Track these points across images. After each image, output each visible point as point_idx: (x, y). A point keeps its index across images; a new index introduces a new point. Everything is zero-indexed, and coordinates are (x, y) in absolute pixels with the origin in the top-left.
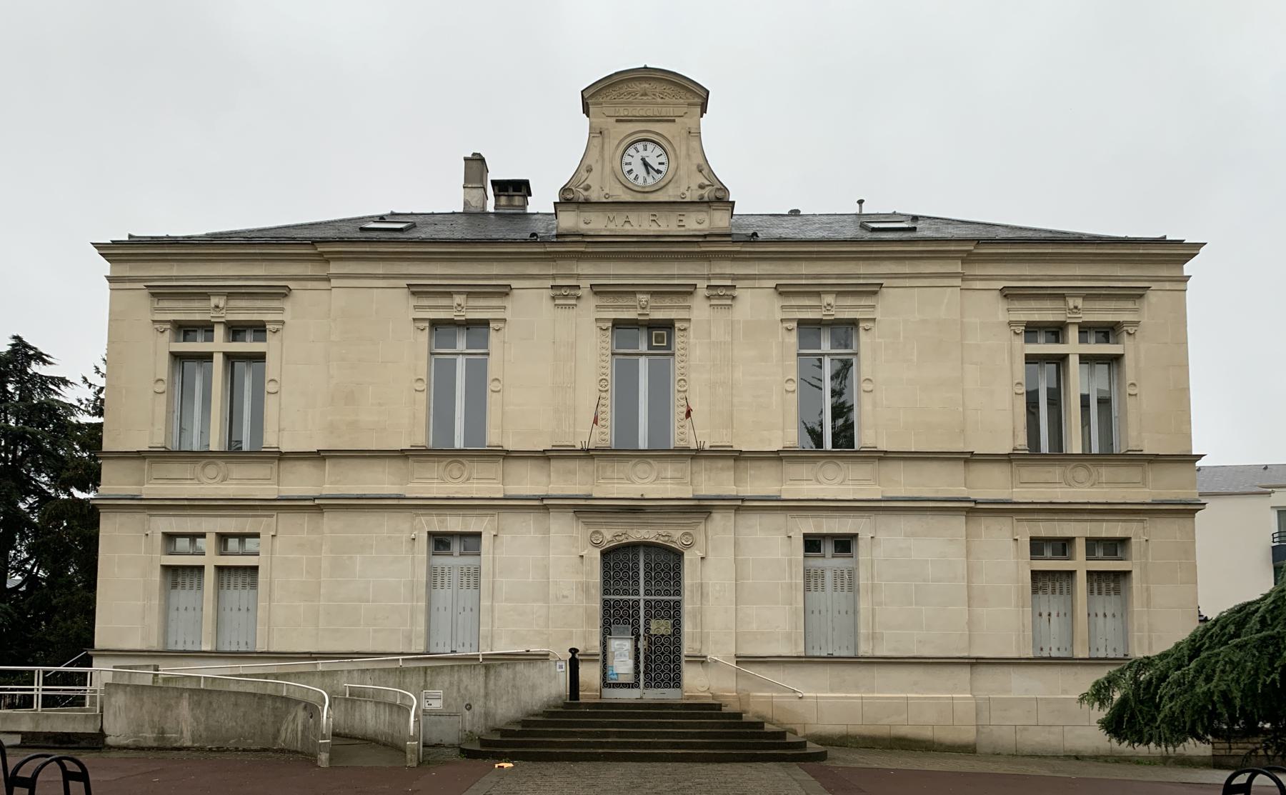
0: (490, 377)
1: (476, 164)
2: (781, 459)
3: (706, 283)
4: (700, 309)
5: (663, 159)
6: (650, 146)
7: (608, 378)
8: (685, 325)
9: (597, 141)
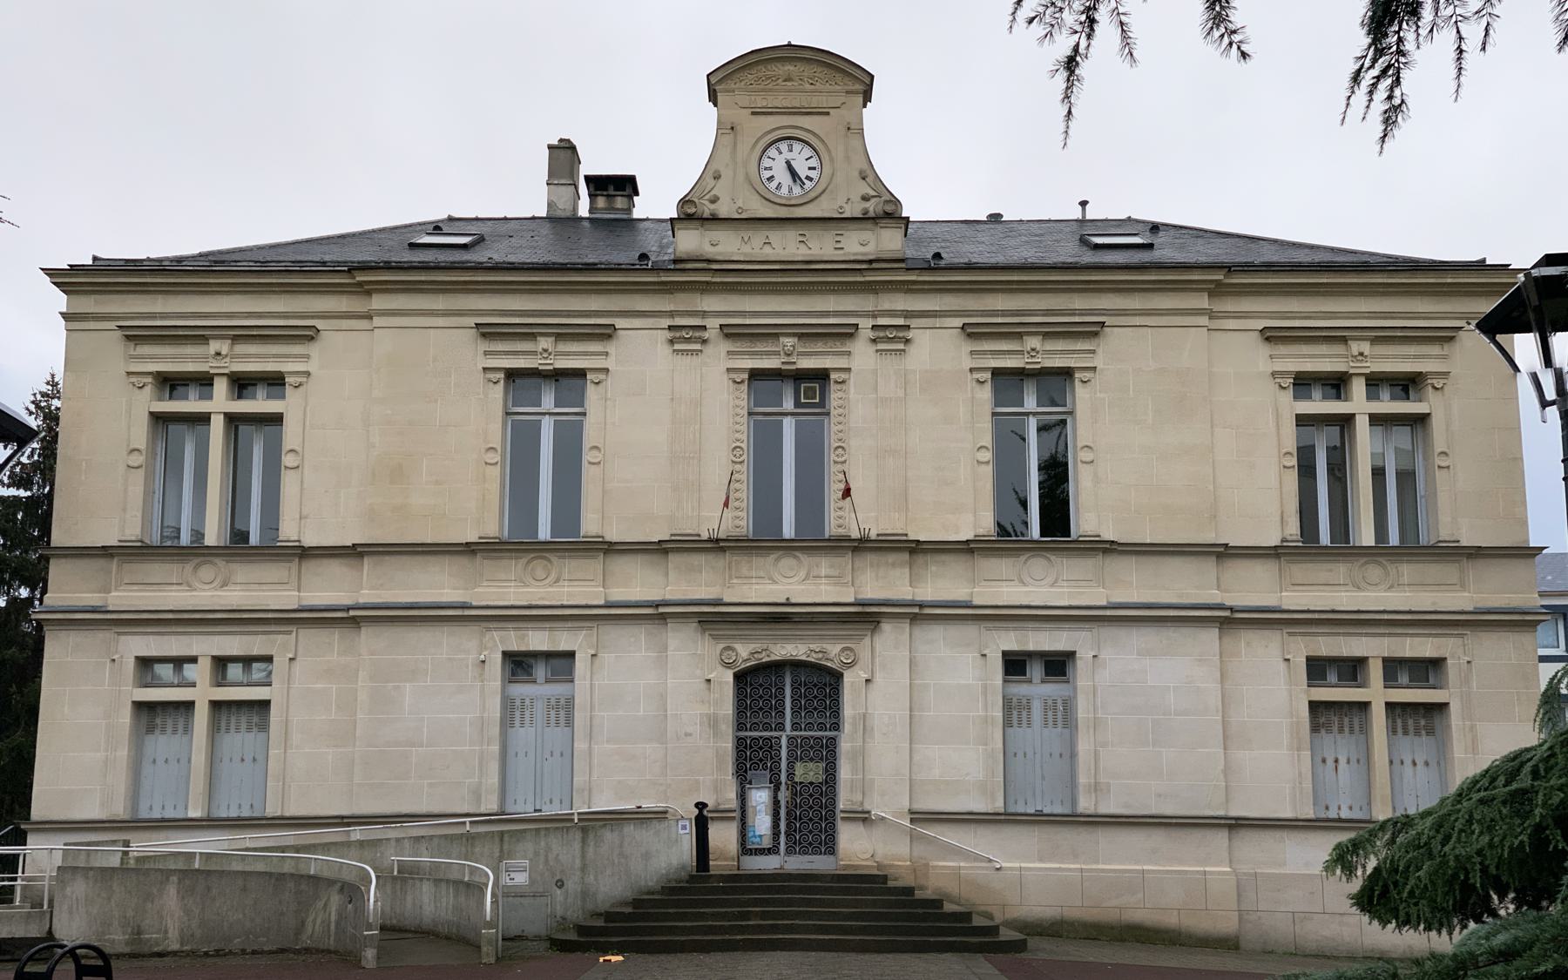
0: (586, 445)
1: (564, 155)
2: (971, 551)
3: (870, 322)
4: (862, 356)
5: (814, 162)
6: (797, 146)
7: (744, 446)
8: (843, 376)
9: (727, 139)
